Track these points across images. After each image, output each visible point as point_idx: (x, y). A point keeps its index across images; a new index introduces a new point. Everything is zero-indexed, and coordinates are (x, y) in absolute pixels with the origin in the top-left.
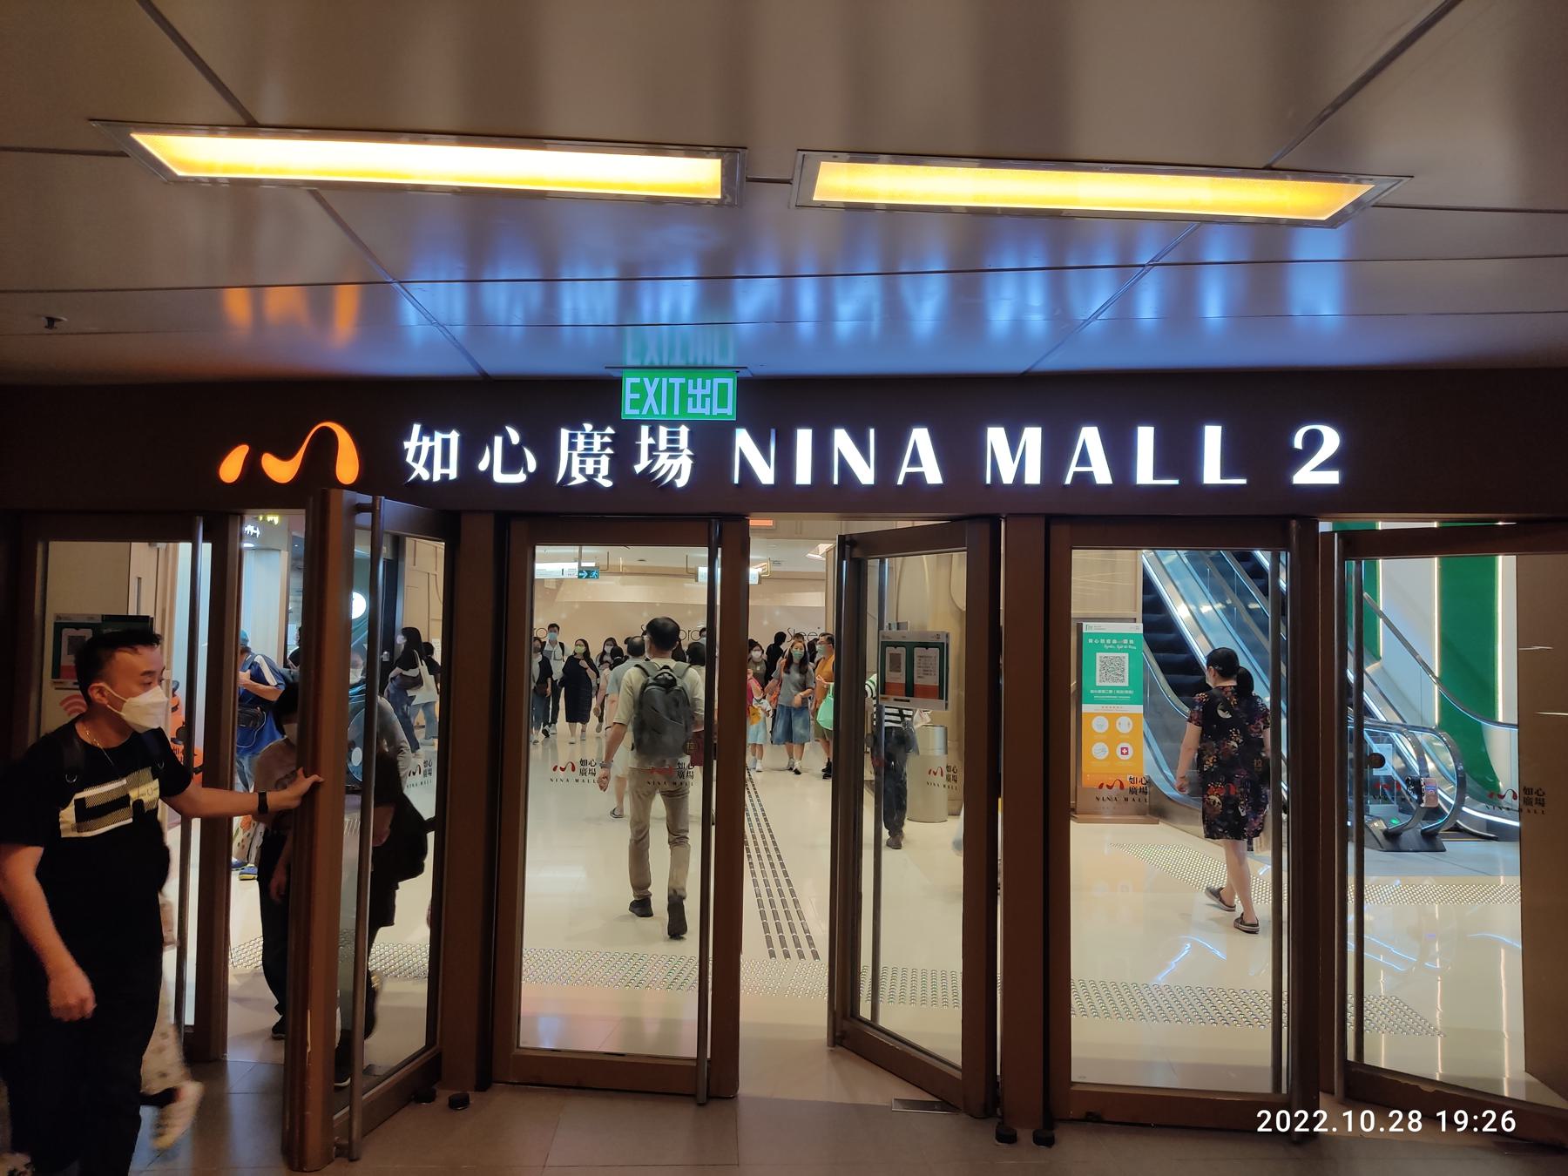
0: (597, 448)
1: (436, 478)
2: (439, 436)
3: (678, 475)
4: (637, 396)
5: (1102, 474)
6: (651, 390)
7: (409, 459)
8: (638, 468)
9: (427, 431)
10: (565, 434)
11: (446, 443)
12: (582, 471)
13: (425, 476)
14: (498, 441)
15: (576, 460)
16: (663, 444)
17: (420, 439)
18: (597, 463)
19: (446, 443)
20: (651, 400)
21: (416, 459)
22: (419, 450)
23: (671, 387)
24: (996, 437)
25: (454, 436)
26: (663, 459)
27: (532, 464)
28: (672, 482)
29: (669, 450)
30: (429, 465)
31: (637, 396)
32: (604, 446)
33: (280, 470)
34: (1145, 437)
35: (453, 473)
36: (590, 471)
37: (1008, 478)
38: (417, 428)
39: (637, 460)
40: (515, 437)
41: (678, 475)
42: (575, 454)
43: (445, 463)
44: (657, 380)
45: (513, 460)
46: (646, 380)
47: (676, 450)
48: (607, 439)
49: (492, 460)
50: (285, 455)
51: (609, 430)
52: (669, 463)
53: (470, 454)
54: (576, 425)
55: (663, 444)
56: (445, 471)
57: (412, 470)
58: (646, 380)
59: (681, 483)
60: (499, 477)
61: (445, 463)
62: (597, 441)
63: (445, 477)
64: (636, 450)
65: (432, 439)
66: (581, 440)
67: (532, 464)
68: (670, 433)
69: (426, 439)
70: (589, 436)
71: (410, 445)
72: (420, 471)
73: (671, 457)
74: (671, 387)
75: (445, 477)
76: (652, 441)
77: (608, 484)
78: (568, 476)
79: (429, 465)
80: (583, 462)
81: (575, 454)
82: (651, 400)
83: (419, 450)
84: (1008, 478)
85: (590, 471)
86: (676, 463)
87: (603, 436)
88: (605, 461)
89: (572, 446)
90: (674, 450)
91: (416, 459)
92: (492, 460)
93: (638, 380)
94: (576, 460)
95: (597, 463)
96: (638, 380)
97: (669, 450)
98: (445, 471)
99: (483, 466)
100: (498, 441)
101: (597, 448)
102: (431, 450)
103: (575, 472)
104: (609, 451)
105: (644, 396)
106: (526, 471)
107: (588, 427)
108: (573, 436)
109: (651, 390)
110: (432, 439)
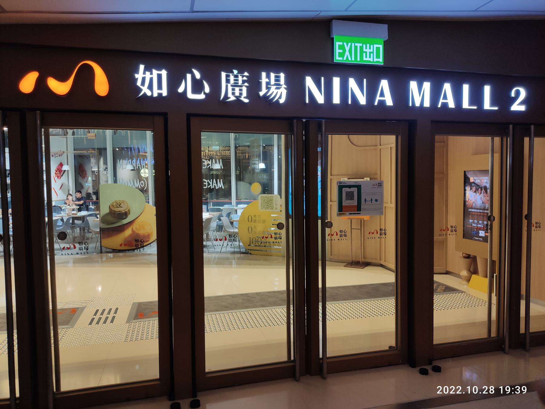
0: (240, 82)
1: (155, 95)
2: (155, 72)
3: (280, 97)
4: (341, 51)
5: (452, 105)
6: (347, 49)
7: (139, 83)
8: (261, 94)
9: (147, 69)
10: (223, 74)
11: (159, 77)
12: (233, 94)
13: (149, 93)
14: (189, 76)
15: (230, 88)
16: (273, 82)
17: (144, 73)
18: (241, 90)
19: (159, 77)
20: (347, 53)
21: (143, 83)
22: (144, 79)
23: (356, 47)
24: (413, 85)
25: (164, 73)
26: (273, 88)
27: (207, 89)
28: (277, 101)
29: (275, 85)
30: (150, 87)
31: (341, 51)
32: (244, 82)
33: (59, 87)
34: (466, 88)
35: (165, 92)
36: (237, 94)
37: (418, 104)
38: (142, 67)
39: (260, 90)
40: (198, 75)
41: (280, 97)
42: (229, 85)
43: (160, 87)
44: (350, 44)
45: (197, 87)
46: (345, 44)
47: (279, 85)
48: (245, 78)
49: (186, 86)
50: (62, 79)
51: (246, 74)
52: (276, 91)
53: (174, 83)
54: (229, 71)
55: (273, 82)
56: (160, 91)
57: (140, 90)
58: (345, 44)
59: (282, 101)
60: (191, 96)
61: (160, 87)
62: (240, 79)
63: (160, 95)
64: (259, 84)
65: (151, 74)
66: (232, 78)
67: (207, 89)
68: (276, 77)
69: (148, 73)
70: (236, 76)
71: (139, 76)
72: (145, 90)
73: (277, 88)
74: (356, 47)
75: (160, 95)
76: (267, 80)
77: (246, 101)
78: (226, 97)
79: (150, 87)
80: (233, 90)
81: (229, 85)
82: (347, 53)
83: (144, 79)
84: (418, 104)
85: (237, 94)
86: (279, 91)
87: (243, 76)
88: (244, 89)
89: (228, 81)
90: (278, 86)
91: (143, 83)
92: (186, 86)
93: (341, 43)
94: (230, 88)
95: (241, 90)
96: (341, 43)
97: (275, 85)
98: (160, 91)
99: (181, 90)
100: (189, 76)
101: (240, 82)
102: (151, 79)
103: (230, 94)
104: (246, 84)
105: (344, 51)
106: (205, 93)
107: (235, 72)
108: (227, 76)
109: (347, 49)
110: (151, 74)
